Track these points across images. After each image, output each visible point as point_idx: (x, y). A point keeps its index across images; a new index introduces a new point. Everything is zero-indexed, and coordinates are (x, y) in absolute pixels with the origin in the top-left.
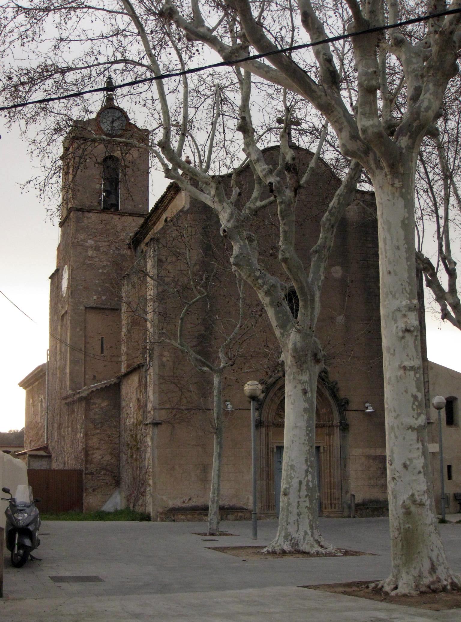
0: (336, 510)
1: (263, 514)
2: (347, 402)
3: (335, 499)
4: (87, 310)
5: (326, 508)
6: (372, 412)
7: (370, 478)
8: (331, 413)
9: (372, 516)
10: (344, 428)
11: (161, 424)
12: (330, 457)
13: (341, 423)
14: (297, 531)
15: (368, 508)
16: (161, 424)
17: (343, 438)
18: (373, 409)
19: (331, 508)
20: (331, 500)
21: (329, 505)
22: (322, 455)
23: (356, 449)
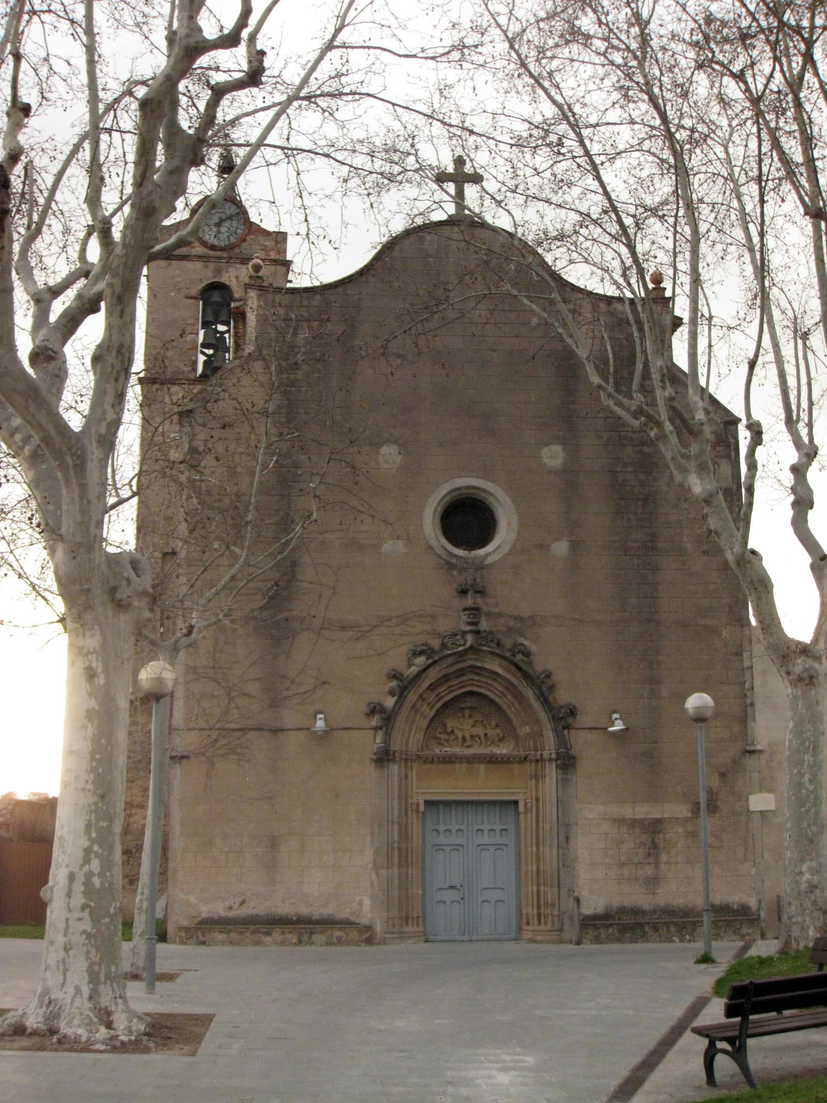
0: (549, 927)
1: (392, 933)
2: (572, 712)
3: (546, 905)
4: (167, 557)
5: (528, 923)
6: (622, 730)
7: (622, 865)
9: (619, 940)
10: (564, 764)
11: (187, 757)
12: (537, 822)
13: (558, 754)
14: (63, 985)
15: (612, 925)
16: (187, 757)
17: (564, 784)
18: (624, 724)
19: (540, 923)
20: (539, 907)
21: (536, 917)
22: (522, 817)
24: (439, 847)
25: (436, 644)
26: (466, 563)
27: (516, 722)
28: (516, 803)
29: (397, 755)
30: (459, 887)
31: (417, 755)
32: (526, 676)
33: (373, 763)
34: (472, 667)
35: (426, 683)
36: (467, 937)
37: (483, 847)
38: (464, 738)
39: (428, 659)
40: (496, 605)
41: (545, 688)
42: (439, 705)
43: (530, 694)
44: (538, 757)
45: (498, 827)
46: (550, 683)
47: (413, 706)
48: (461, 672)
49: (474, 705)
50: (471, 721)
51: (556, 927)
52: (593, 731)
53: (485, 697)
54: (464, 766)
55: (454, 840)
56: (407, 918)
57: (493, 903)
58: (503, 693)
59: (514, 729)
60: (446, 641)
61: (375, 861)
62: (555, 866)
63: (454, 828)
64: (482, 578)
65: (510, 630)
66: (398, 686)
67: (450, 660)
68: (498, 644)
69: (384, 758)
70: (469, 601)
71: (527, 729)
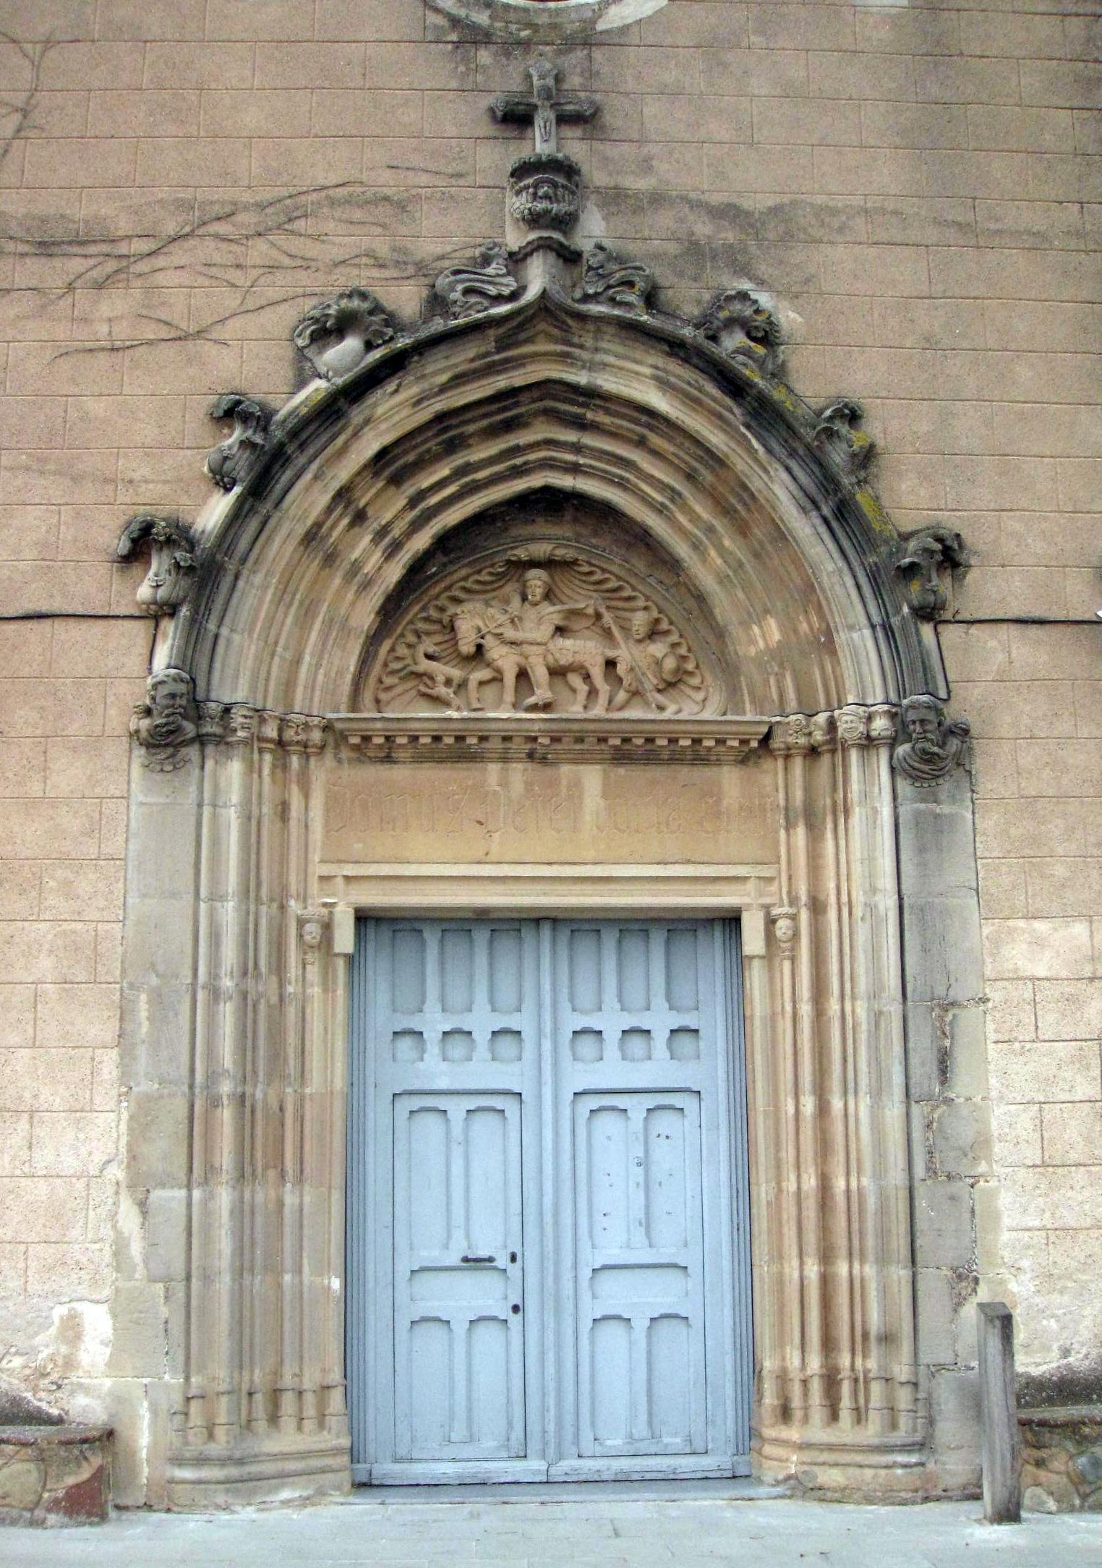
0: (872, 1431)
1: (201, 1461)
2: (949, 556)
3: (861, 1340)
5: (785, 1413)
10: (928, 758)
17: (923, 838)
20: (828, 1344)
21: (816, 1387)
22: (756, 977)
23: (1041, 926)
24: (426, 1102)
25: (405, 299)
26: (530, 25)
27: (724, 605)
28: (731, 921)
29: (237, 719)
30: (502, 1261)
31: (327, 728)
32: (766, 416)
34: (544, 386)
35: (370, 445)
36: (533, 1467)
37: (606, 1100)
38: (523, 675)
39: (369, 346)
40: (646, 166)
41: (838, 456)
42: (422, 541)
43: (779, 488)
44: (819, 736)
45: (661, 1021)
46: (859, 439)
47: (312, 537)
48: (505, 411)
49: (560, 553)
50: (552, 613)
51: (901, 1436)
52: (1033, 631)
53: (604, 513)
54: (519, 773)
55: (482, 1071)
56: (275, 1395)
57: (641, 1324)
58: (674, 494)
59: (720, 634)
60: (442, 282)
61: (133, 1157)
62: (897, 1177)
63: (482, 1022)
64: (591, 73)
65: (695, 251)
66: (245, 444)
67: (463, 356)
68: (651, 299)
69: (180, 727)
70: (540, 143)
71: (773, 631)
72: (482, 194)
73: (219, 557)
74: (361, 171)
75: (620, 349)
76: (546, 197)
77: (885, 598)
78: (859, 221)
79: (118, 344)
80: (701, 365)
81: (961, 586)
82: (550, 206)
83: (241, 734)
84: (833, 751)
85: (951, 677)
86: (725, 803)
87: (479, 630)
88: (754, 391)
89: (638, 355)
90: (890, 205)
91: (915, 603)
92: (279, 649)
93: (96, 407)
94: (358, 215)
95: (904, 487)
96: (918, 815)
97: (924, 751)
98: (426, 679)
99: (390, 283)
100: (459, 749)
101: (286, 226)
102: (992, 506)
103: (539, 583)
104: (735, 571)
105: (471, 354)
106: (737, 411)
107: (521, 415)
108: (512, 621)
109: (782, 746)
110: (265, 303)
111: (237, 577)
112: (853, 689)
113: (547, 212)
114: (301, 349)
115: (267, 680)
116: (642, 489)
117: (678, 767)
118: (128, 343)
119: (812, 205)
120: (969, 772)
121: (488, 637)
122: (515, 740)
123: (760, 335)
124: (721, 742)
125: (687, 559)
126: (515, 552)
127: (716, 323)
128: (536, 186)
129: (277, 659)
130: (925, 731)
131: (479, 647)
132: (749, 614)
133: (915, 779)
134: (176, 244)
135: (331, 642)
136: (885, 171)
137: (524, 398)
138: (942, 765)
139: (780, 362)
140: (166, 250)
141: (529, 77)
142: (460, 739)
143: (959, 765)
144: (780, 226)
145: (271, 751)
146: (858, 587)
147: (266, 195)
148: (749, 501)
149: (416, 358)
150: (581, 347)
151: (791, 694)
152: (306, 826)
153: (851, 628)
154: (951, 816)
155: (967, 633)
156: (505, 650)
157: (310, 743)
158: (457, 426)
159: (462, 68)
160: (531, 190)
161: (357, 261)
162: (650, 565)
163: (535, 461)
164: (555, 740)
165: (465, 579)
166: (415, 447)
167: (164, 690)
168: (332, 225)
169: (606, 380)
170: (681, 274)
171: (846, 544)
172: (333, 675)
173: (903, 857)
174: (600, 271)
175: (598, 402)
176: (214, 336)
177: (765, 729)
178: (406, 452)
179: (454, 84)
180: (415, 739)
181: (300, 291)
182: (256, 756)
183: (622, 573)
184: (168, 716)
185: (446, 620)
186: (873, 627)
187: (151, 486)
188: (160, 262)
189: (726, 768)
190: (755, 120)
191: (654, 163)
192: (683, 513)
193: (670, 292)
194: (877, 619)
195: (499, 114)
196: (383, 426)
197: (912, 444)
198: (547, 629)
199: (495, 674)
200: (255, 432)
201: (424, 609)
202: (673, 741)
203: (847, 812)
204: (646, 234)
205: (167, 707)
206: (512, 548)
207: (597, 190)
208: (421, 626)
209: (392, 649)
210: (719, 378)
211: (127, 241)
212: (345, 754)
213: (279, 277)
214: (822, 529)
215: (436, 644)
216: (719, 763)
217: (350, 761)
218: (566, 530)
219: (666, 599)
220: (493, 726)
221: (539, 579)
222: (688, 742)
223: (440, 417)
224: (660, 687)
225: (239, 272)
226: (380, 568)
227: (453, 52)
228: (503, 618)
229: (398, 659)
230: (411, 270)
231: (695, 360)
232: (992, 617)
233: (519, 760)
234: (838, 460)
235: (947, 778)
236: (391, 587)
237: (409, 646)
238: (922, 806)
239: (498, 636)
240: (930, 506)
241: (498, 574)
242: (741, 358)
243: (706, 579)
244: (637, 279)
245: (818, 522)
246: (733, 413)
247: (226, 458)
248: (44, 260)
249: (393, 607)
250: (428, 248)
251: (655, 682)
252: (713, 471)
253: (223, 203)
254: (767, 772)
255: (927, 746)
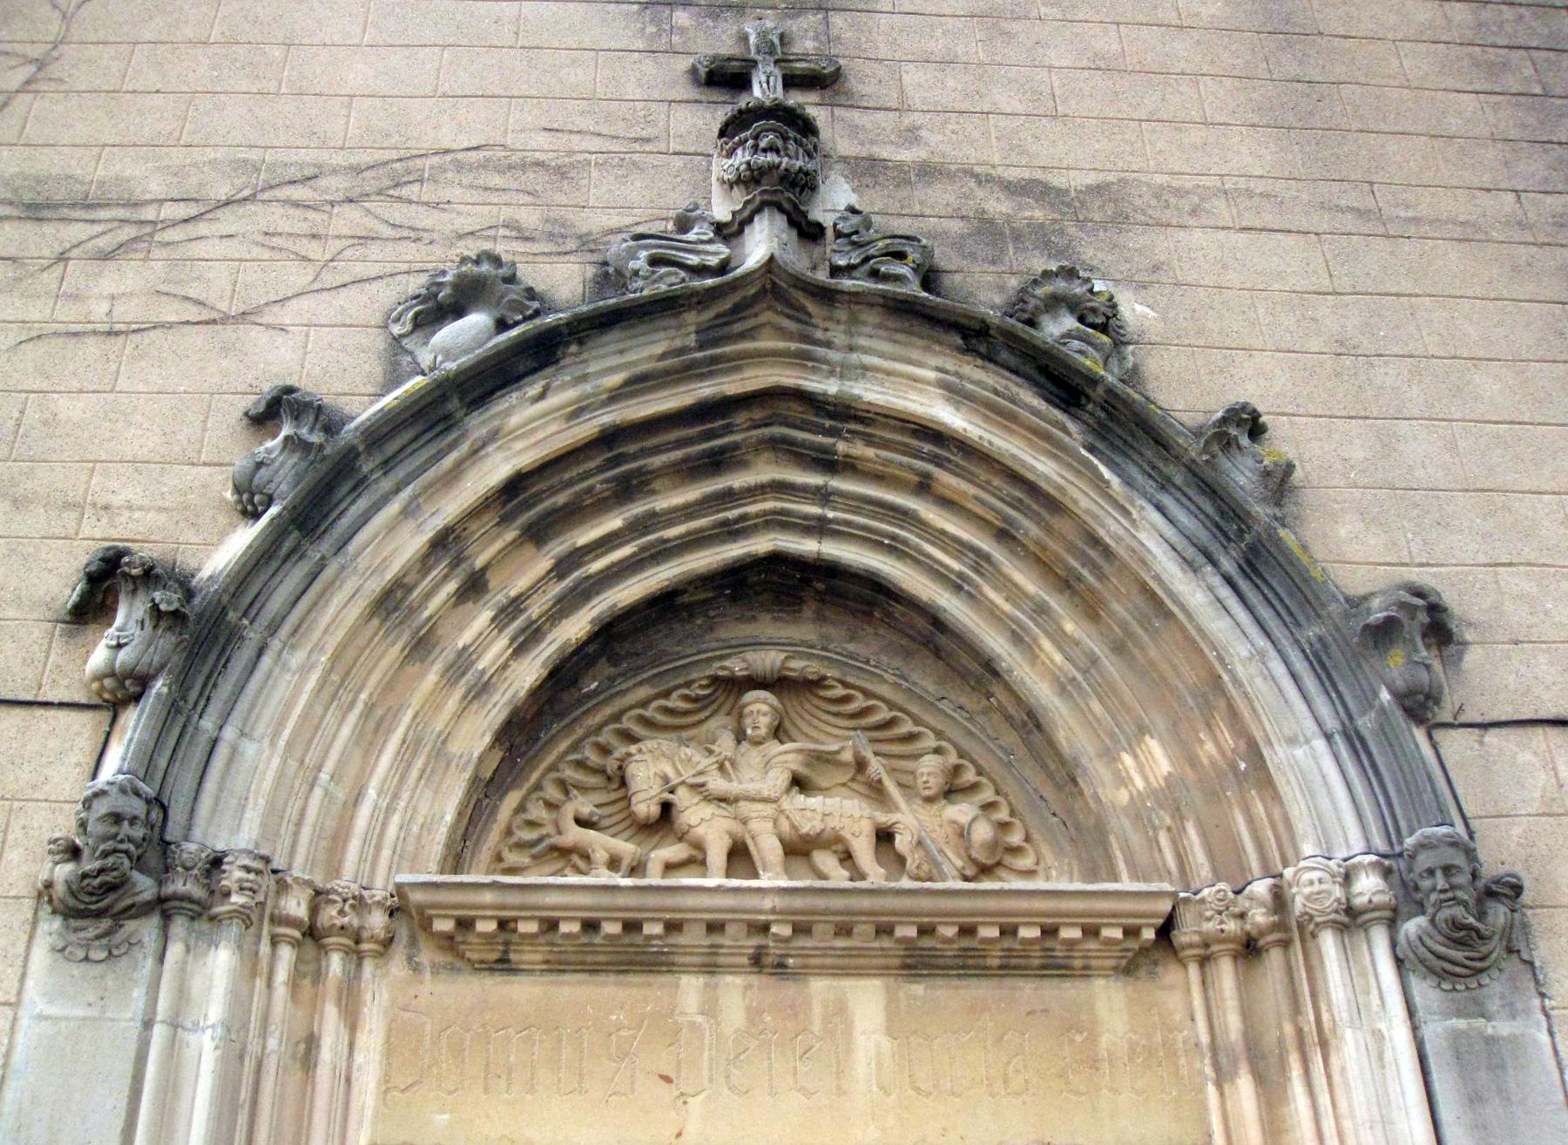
8: (1255, 772)
27: (1071, 730)
29: (233, 875)
33: (51, 925)
35: (496, 469)
38: (740, 856)
39: (502, 325)
40: (911, 136)
41: (1241, 475)
42: (576, 627)
43: (1151, 535)
44: (1260, 917)
47: (391, 602)
50: (786, 757)
53: (867, 598)
58: (981, 560)
59: (1066, 775)
65: (988, 231)
67: (647, 349)
69: (125, 884)
71: (1156, 760)
72: (678, 162)
73: (232, 616)
74: (506, 132)
75: (886, 347)
76: (772, 148)
77: (1342, 688)
78: (1220, 205)
79: (117, 327)
80: (1013, 361)
81: (1459, 671)
82: (777, 160)
83: (237, 899)
84: (1286, 944)
85: (1469, 810)
86: (1104, 1041)
87: (666, 779)
88: (1100, 390)
89: (915, 355)
90: (1260, 187)
91: (1400, 684)
92: (324, 776)
93: (70, 408)
94: (497, 180)
95: (1343, 532)
96: (1456, 1040)
97: (1456, 925)
98: (575, 858)
99: (540, 259)
100: (628, 947)
101: (391, 192)
102: (1482, 559)
103: (765, 708)
104: (1084, 672)
105: (659, 349)
106: (1072, 426)
107: (735, 446)
108: (721, 768)
109: (1196, 938)
110: (348, 279)
111: (260, 652)
112: (1312, 838)
113: (774, 167)
114: (397, 339)
115: (299, 825)
116: (925, 554)
117: (1020, 983)
118: (134, 327)
119: (1148, 185)
120: (1530, 963)
121: (682, 792)
122: (731, 930)
123: (1100, 320)
124: (1091, 932)
125: (1005, 655)
126: (727, 663)
127: (1033, 302)
128: (756, 138)
129: (318, 792)
130: (1453, 887)
131: (667, 807)
132: (1112, 735)
133: (1441, 975)
134: (226, 210)
135: (414, 774)
136: (1244, 150)
137: (741, 418)
138: (1484, 949)
139: (1130, 365)
140: (209, 216)
141: (744, 38)
142: (632, 926)
143: (1510, 951)
144: (1111, 204)
145: (297, 944)
146: (1294, 676)
147: (366, 158)
148: (1100, 560)
149: (573, 348)
150: (828, 344)
151: (1199, 856)
152: (348, 1080)
153: (1292, 741)
154: (1513, 1039)
155: (1481, 743)
156: (708, 810)
157: (365, 935)
158: (635, 457)
159: (651, 29)
160: (750, 142)
161: (492, 232)
162: (941, 681)
163: (757, 515)
164: (801, 929)
165: (644, 704)
166: (570, 483)
167: (101, 807)
168: (458, 191)
169: (866, 390)
170: (972, 256)
171: (1265, 613)
172: (415, 829)
173: (1446, 1113)
174: (854, 238)
175: (852, 426)
176: (266, 319)
177: (1165, 906)
178: (553, 491)
179: (640, 45)
180: (551, 925)
181: (405, 267)
182: (265, 948)
183: (898, 698)
184: (105, 854)
185: (611, 764)
186: (1328, 737)
187: (137, 515)
188: (202, 228)
189: (1099, 983)
190: (1057, 93)
191: (923, 133)
192: (996, 589)
193: (958, 278)
194: (1332, 724)
195: (703, 71)
196: (519, 445)
197: (1345, 475)
198: (777, 780)
199: (694, 853)
200: (312, 430)
201: (575, 747)
202: (1008, 931)
203: (1324, 1044)
204: (917, 209)
205: (105, 839)
206: (721, 658)
207: (844, 159)
208: (569, 773)
209: (521, 808)
210: (1042, 380)
211: (155, 205)
212: (426, 955)
213: (374, 250)
214: (1225, 592)
215: (597, 806)
216: (1086, 973)
217: (436, 969)
218: (804, 631)
219: (971, 734)
220: (690, 901)
221: (765, 702)
222: (1035, 933)
223: (610, 438)
224: (969, 872)
225: (314, 244)
226: (505, 666)
227: (639, 13)
228: (704, 762)
229: (532, 824)
230: (571, 244)
231: (1004, 355)
232: (1516, 718)
233: (733, 969)
234: (1242, 480)
235: (1495, 973)
236: (522, 693)
237: (551, 806)
238: (1461, 1024)
239: (697, 787)
240: (1388, 559)
241: (696, 700)
242: (1076, 344)
243: (1041, 691)
244: (908, 249)
245: (1216, 581)
246: (1069, 434)
247: (259, 465)
248: (29, 225)
249: (522, 734)
250: (596, 221)
251: (959, 863)
252: (1039, 520)
253: (301, 166)
254: (1172, 987)
255: (1458, 912)
